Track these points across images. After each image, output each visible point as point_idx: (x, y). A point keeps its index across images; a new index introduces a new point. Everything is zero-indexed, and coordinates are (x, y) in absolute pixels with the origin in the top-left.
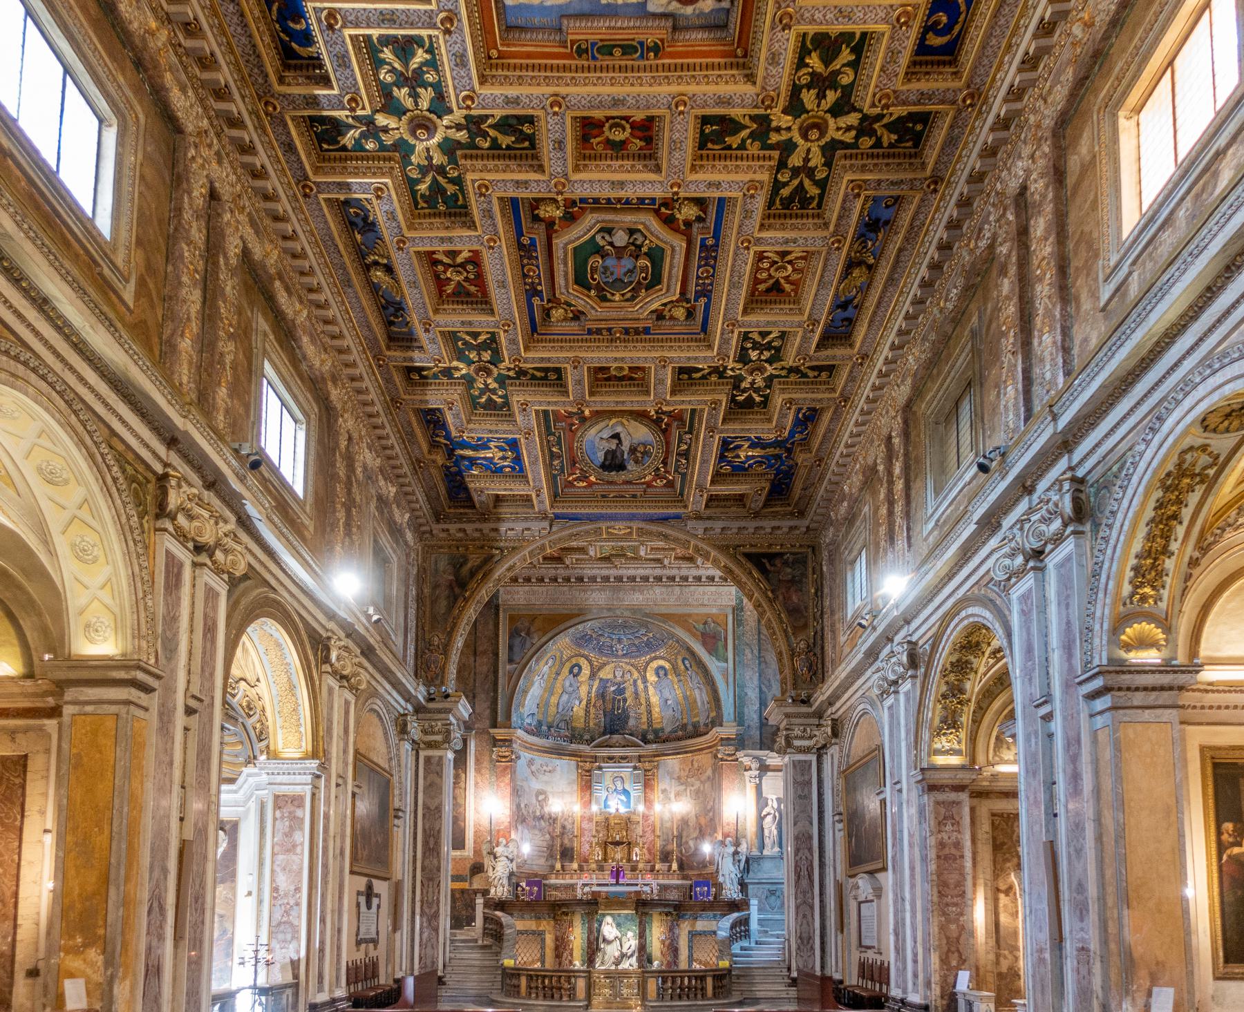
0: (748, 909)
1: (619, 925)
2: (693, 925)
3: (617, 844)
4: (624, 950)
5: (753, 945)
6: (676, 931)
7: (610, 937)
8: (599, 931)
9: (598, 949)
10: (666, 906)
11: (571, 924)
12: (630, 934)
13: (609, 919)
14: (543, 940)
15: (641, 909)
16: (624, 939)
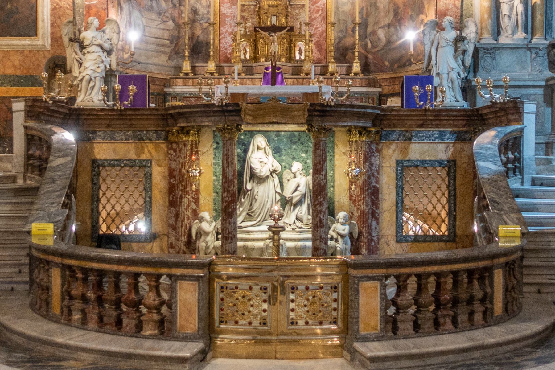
0: (520, 120)
1: (277, 151)
2: (404, 151)
3: (274, 29)
4: (287, 193)
5: (527, 186)
6: (376, 161)
7: (263, 170)
8: (243, 160)
9: (241, 191)
10: (361, 116)
11: (195, 149)
12: (297, 166)
13: (260, 140)
14: (148, 177)
15: (317, 122)
16: (287, 175)
